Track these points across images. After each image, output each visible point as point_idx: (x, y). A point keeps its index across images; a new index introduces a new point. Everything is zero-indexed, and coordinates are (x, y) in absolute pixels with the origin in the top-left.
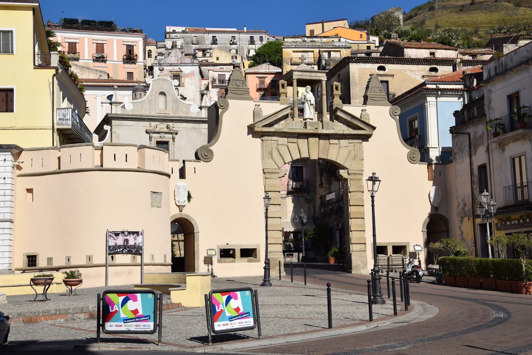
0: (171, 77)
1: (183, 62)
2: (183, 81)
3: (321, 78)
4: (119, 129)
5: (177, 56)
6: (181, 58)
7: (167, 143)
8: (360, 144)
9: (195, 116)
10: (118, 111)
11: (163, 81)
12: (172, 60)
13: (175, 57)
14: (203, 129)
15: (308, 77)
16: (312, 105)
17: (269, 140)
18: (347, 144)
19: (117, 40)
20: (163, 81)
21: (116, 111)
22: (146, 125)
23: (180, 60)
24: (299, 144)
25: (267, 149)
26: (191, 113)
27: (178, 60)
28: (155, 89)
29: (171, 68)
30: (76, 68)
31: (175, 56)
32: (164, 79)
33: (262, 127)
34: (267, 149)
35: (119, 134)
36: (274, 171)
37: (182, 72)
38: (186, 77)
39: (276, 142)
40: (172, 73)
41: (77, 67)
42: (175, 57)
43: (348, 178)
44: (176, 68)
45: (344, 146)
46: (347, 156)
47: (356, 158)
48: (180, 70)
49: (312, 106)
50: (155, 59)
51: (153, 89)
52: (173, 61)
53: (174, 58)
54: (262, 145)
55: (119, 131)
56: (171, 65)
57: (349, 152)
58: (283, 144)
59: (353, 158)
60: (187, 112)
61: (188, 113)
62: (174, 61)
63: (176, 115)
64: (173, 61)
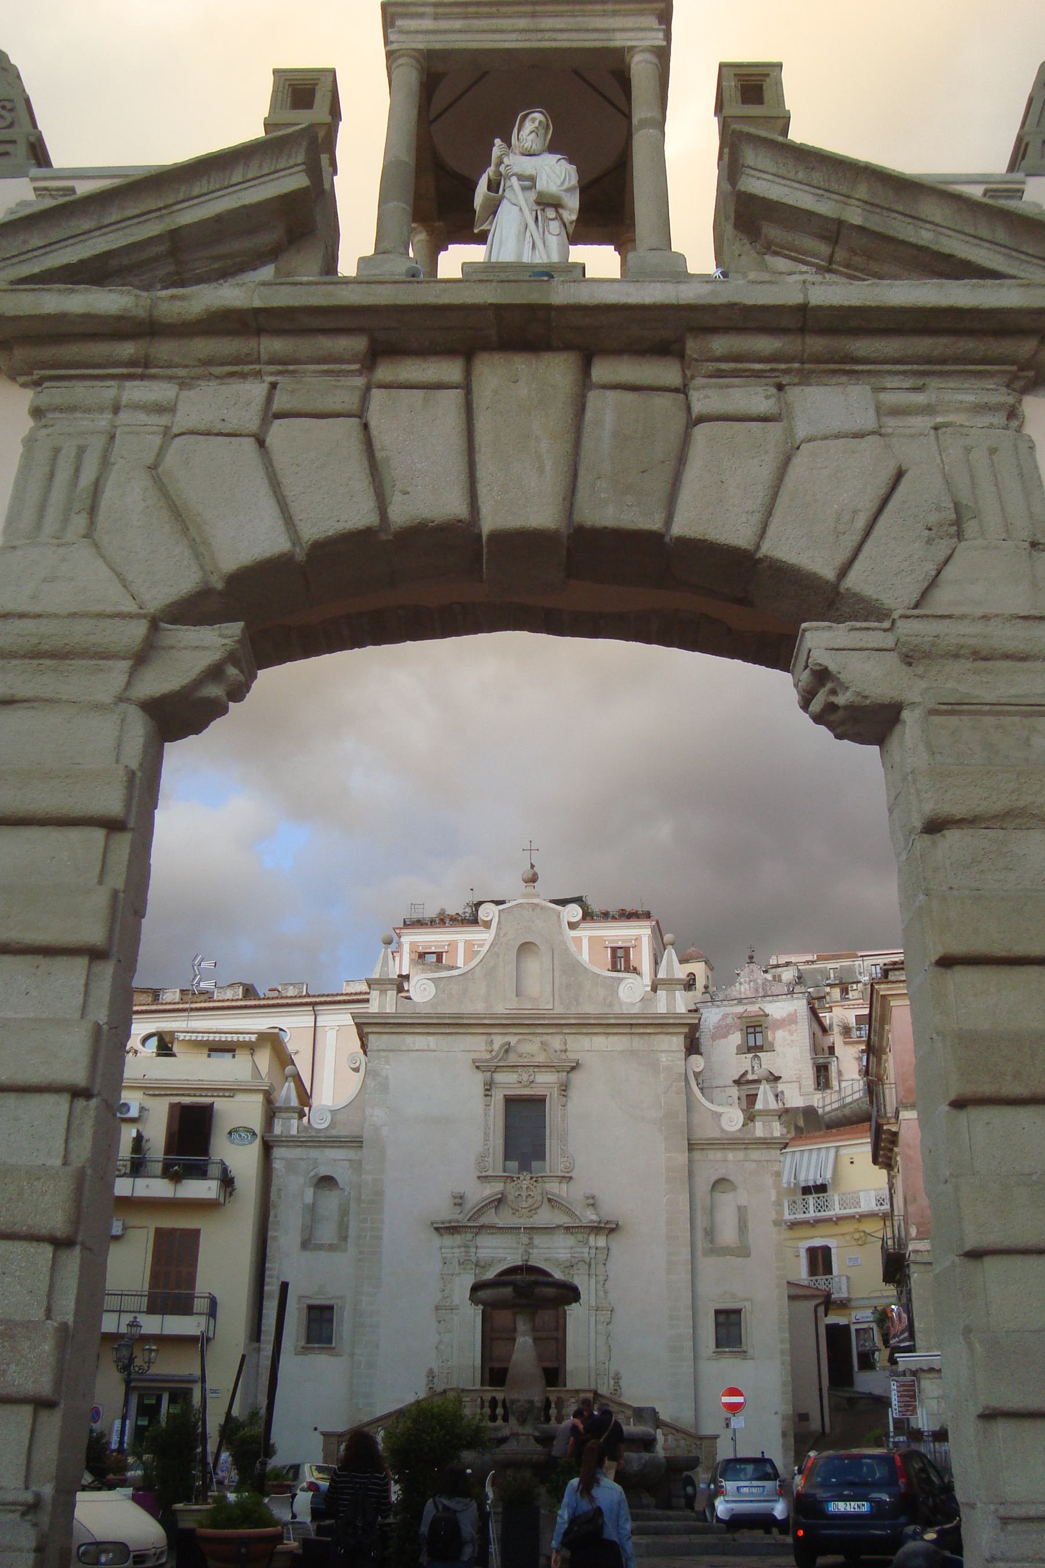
0: (741, 1030)
1: (769, 993)
2: (770, 1038)
3: (619, 41)
4: (387, 1063)
5: (755, 981)
6: (763, 983)
7: (539, 1102)
8: (999, 419)
9: (635, 1010)
10: (387, 1006)
11: (533, 910)
12: (743, 990)
13: (749, 984)
14: (663, 1055)
15: (514, 36)
16: (557, 205)
17: (101, 410)
18: (867, 420)
19: (590, 938)
20: (533, 910)
21: (382, 1005)
22: (475, 1045)
23: (760, 990)
24: (373, 424)
25: (63, 475)
26: (621, 1004)
27: (757, 990)
28: (505, 935)
29: (740, 1009)
30: (423, 970)
31: (751, 981)
32: (537, 905)
33: (12, 283)
34: (63, 475)
35: (387, 1078)
36: (80, 633)
37: (767, 1015)
38: (779, 1028)
39: (164, 420)
40: (744, 1020)
41: (425, 967)
42: (749, 984)
43: (913, 696)
44: (753, 1009)
45: (837, 424)
46: (867, 505)
47: (971, 527)
48: (762, 1013)
49: (551, 213)
50: (703, 993)
51: (501, 935)
52: (745, 993)
53: (747, 986)
54: (30, 442)
55: (387, 1067)
56: (740, 1001)
57: (886, 475)
58: (219, 427)
59: (933, 519)
60: (608, 1001)
61: (611, 1005)
62: (748, 992)
63: (573, 1010)
64: (745, 993)
